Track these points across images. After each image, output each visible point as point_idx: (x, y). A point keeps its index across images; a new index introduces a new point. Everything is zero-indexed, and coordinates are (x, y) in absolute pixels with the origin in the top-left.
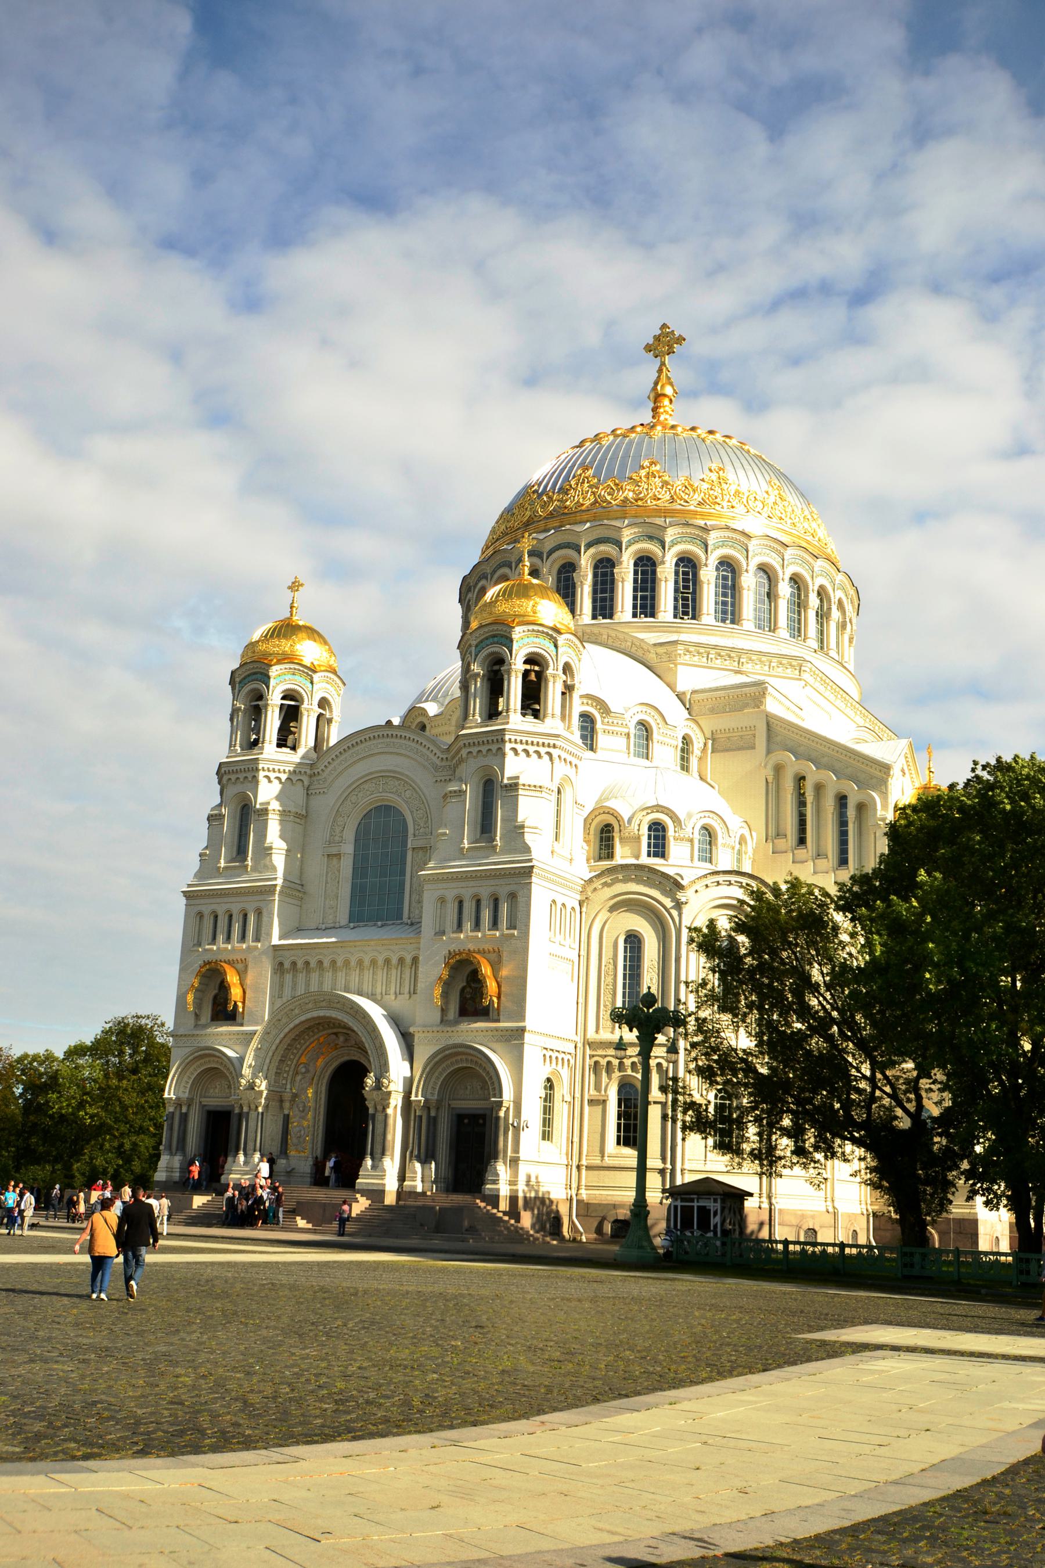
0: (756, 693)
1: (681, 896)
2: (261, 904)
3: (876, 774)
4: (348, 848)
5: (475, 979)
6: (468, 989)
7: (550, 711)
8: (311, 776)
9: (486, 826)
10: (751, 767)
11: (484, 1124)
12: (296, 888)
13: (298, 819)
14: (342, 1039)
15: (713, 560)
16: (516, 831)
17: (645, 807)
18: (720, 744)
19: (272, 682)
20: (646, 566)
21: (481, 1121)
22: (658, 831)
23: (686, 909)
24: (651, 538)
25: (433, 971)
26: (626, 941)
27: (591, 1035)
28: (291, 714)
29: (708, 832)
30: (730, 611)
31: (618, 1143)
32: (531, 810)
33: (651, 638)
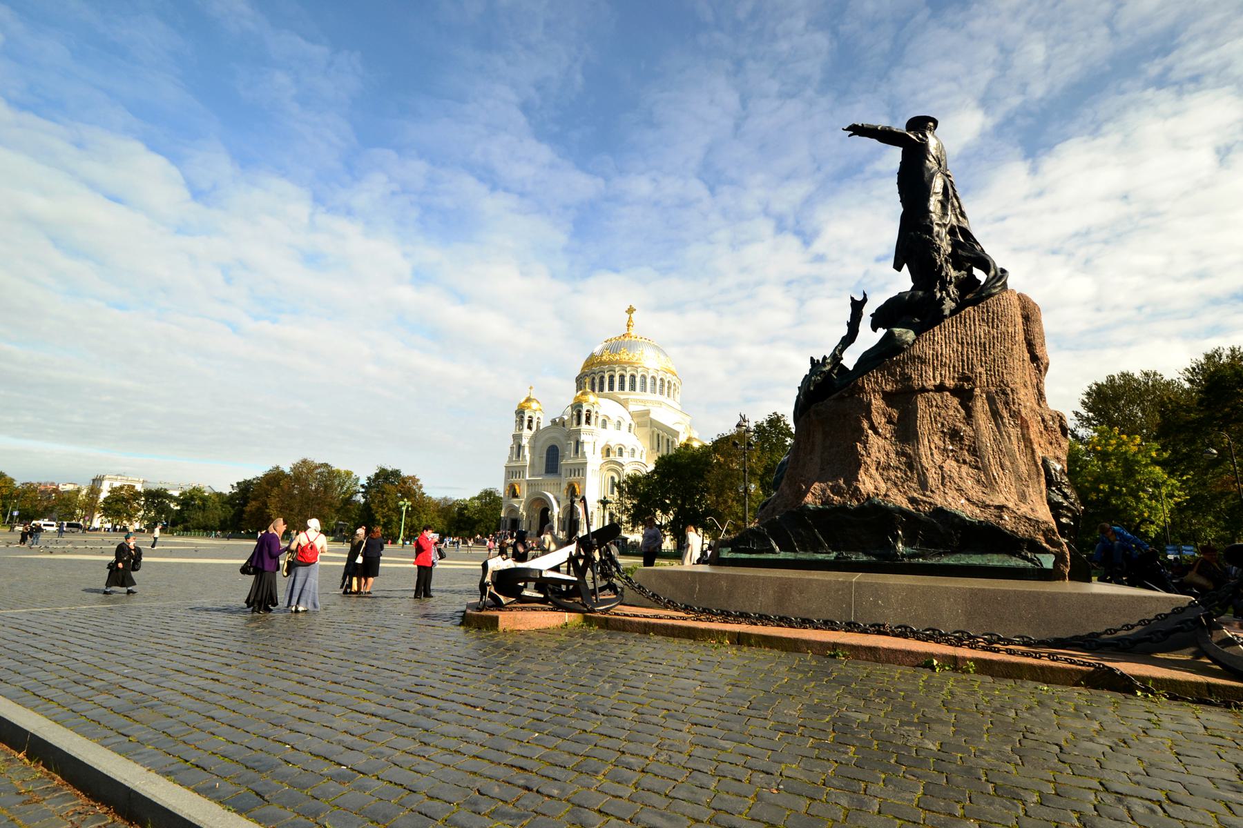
0: (647, 413)
3: (676, 434)
5: (574, 489)
9: (577, 452)
10: (647, 429)
12: (532, 465)
13: (532, 448)
16: (584, 453)
17: (617, 448)
18: (639, 425)
20: (622, 377)
22: (620, 450)
25: (565, 486)
28: (530, 421)
30: (644, 389)
32: (587, 448)
33: (622, 397)
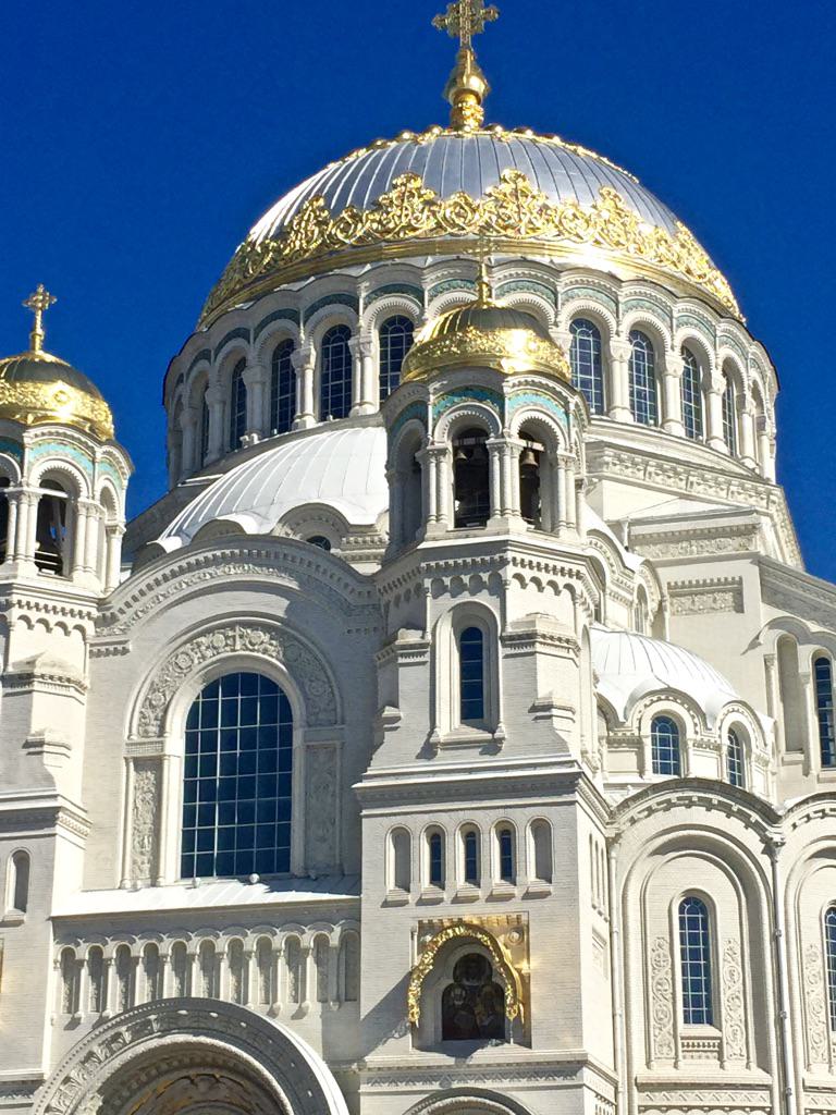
1: (773, 833)
2: (29, 846)
4: (175, 745)
6: (458, 991)
7: (563, 517)
8: (97, 624)
14: (203, 1087)
15: (625, 328)
19: (29, 455)
22: (666, 727)
23: (782, 855)
24: (533, 284)
25: (391, 955)
26: (681, 911)
27: (640, 1072)
28: (56, 518)
29: (737, 735)
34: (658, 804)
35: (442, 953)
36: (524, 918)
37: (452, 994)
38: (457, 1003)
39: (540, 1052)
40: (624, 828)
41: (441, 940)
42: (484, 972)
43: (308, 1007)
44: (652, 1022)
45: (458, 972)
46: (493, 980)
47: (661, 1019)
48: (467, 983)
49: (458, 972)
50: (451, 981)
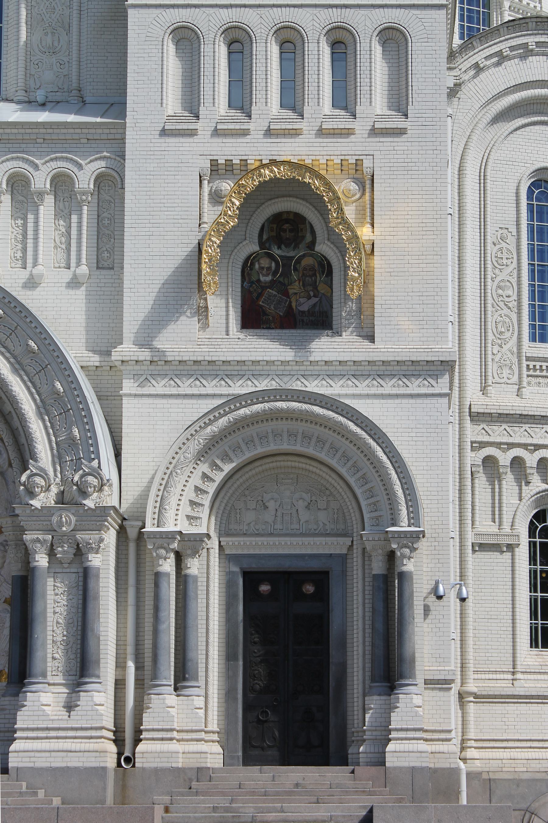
6: (265, 262)
11: (323, 594)
21: (309, 588)
25: (173, 210)
31: (534, 643)
34: (512, 48)
35: (251, 201)
36: (367, 163)
37: (257, 266)
38: (262, 278)
39: (389, 345)
40: (466, 77)
41: (251, 184)
42: (303, 237)
43: (42, 276)
44: (490, 337)
45: (265, 237)
46: (318, 248)
47: (501, 333)
48: (276, 252)
49: (265, 237)
50: (256, 248)
